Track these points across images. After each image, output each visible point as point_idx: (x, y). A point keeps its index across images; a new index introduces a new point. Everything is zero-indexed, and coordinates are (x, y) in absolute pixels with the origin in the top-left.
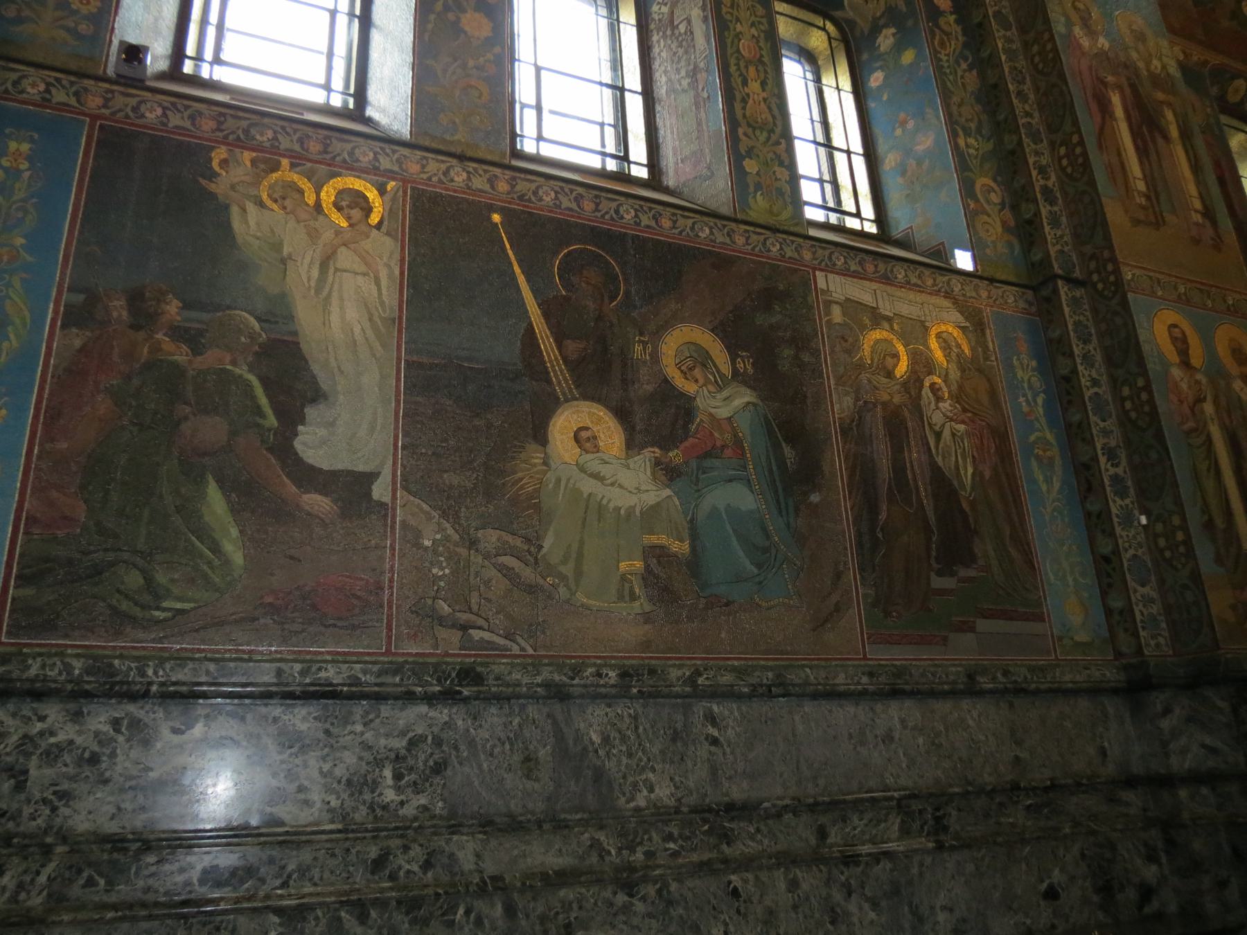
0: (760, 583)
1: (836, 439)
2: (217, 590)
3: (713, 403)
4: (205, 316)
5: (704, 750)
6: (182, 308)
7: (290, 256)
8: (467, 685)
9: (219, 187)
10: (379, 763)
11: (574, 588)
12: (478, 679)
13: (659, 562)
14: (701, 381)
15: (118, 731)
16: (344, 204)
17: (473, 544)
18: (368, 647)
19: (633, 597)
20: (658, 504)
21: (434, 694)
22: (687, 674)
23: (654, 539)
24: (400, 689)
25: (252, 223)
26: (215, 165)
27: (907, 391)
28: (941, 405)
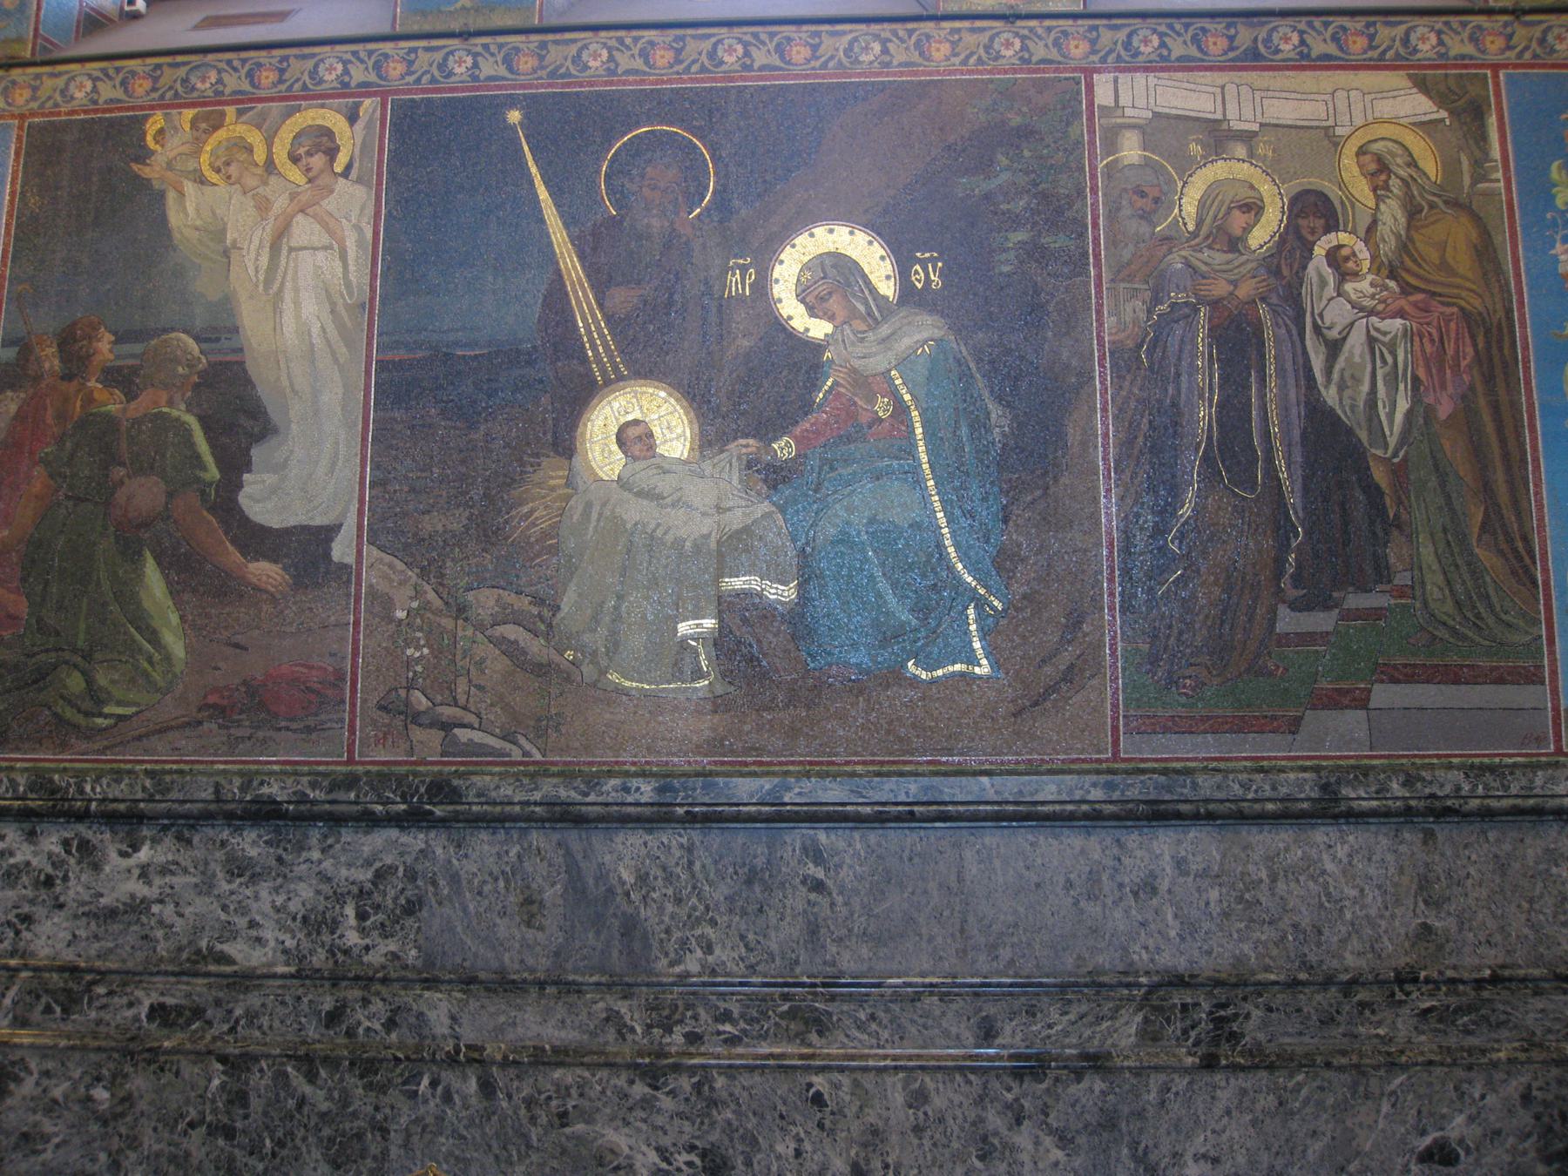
1: (1101, 378)
2: (157, 690)
3: (860, 350)
4: (138, 348)
5: (798, 899)
6: (115, 343)
7: (234, 245)
8: (441, 803)
9: (152, 171)
10: (340, 898)
11: (604, 663)
12: (454, 796)
14: (841, 315)
15: (68, 852)
16: (302, 151)
17: (461, 611)
19: (698, 674)
20: (746, 530)
21: (398, 814)
22: (767, 787)
23: (737, 583)
24: (356, 808)
25: (190, 209)
27: (1277, 273)
28: (1349, 287)
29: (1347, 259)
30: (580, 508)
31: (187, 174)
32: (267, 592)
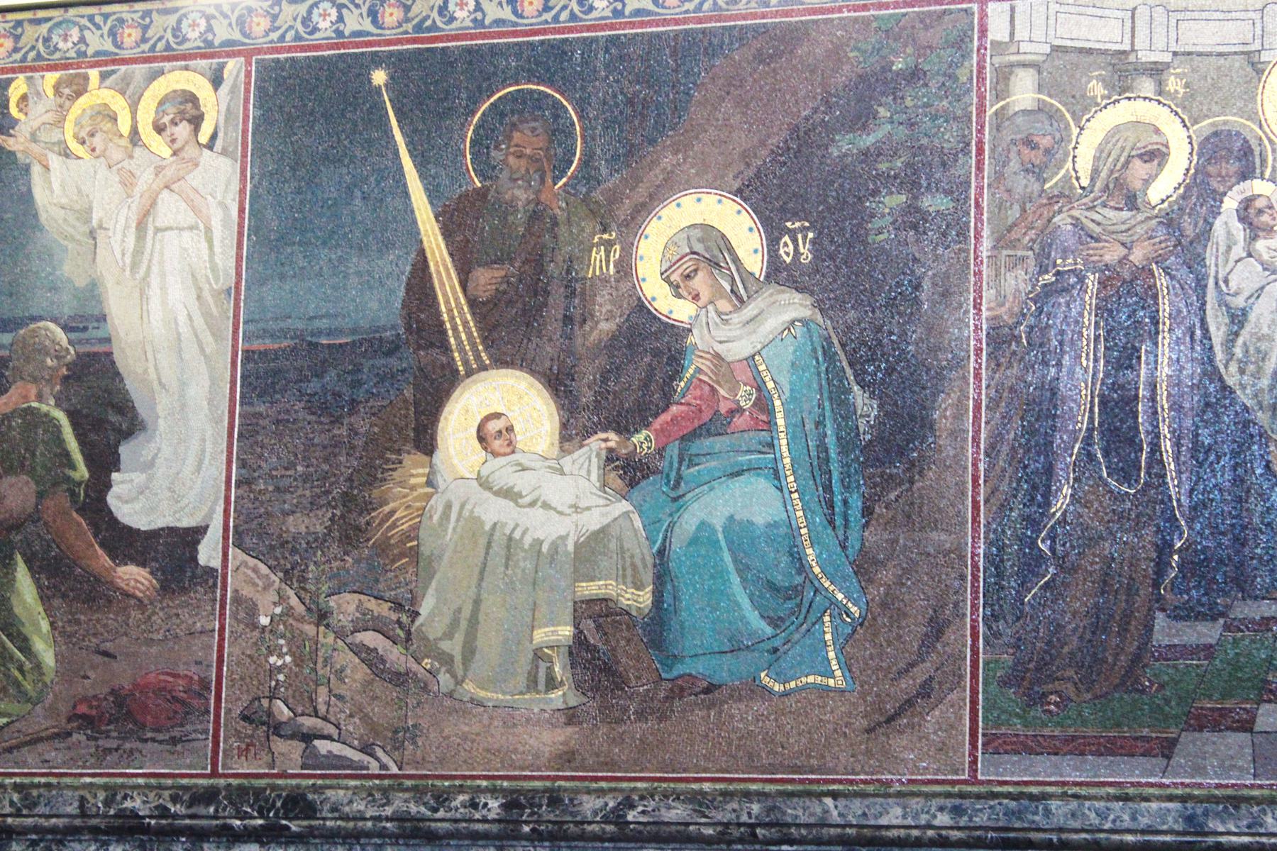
0: (775, 650)
1: (977, 363)
2: (29, 700)
3: (721, 333)
8: (296, 818)
9: (16, 143)
11: (460, 673)
12: (309, 810)
13: (599, 627)
16: (166, 119)
17: (322, 617)
18: (189, 767)
19: (551, 684)
20: (603, 530)
21: (255, 828)
22: (611, 804)
23: (590, 589)
24: (215, 822)
25: (56, 186)
26: (14, 111)
28: (1260, 245)
29: (1260, 212)
30: (440, 509)
31: (50, 146)
32: (134, 597)
